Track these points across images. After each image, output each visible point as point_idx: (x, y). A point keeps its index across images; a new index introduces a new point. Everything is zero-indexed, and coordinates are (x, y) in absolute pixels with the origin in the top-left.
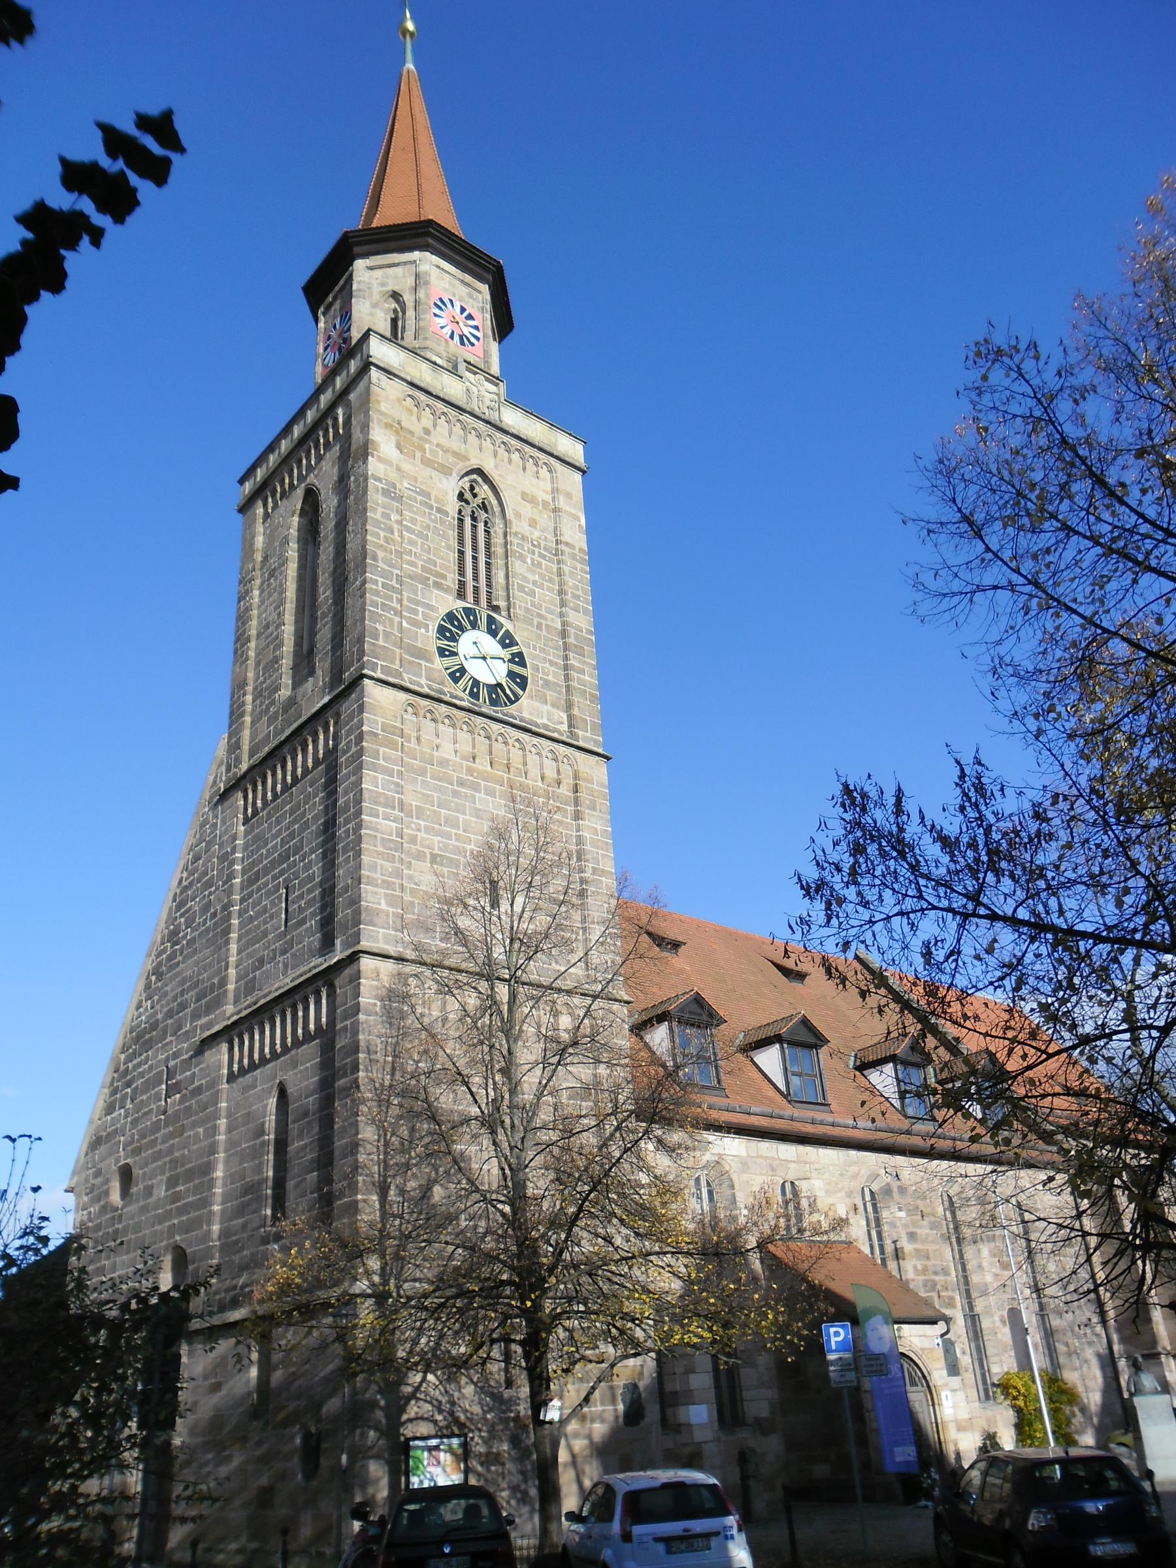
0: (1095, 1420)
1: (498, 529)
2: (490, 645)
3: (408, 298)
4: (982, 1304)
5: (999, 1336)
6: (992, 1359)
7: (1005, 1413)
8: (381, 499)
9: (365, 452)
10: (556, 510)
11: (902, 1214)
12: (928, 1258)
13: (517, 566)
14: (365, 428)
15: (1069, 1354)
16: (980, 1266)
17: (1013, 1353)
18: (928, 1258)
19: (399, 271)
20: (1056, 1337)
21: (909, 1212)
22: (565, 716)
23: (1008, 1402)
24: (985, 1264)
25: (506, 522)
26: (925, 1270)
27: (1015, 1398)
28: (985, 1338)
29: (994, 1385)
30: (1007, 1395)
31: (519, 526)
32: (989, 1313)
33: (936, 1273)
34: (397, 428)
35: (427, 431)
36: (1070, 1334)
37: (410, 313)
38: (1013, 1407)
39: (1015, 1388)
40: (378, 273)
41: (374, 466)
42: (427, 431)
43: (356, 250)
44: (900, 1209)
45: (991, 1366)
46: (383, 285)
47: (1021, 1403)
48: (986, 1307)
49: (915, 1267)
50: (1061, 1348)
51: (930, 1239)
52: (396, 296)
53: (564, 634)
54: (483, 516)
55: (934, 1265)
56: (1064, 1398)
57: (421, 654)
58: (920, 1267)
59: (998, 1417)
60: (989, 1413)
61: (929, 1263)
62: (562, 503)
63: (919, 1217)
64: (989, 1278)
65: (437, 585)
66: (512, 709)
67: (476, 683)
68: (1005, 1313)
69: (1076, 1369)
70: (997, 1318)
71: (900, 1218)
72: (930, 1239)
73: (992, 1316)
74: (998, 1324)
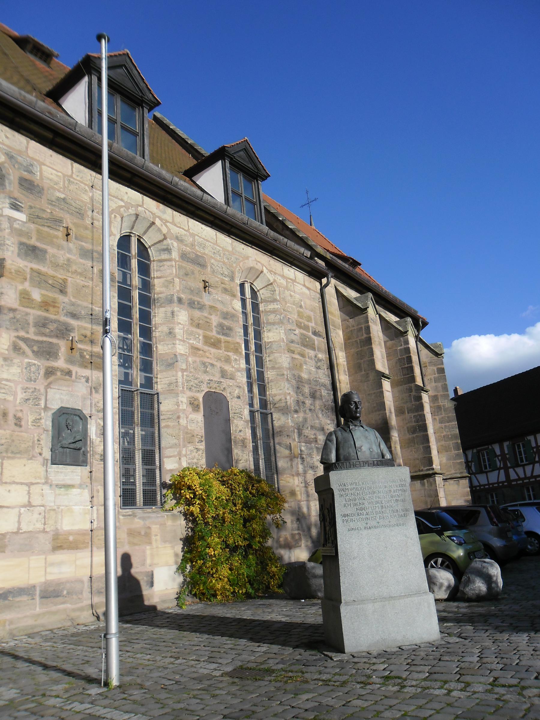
0: (314, 532)
4: (166, 381)
5: (183, 422)
6: (166, 452)
7: (169, 523)
11: (21, 217)
12: (63, 291)
15: (292, 458)
16: (171, 333)
17: (202, 446)
18: (63, 291)
20: (277, 440)
21: (34, 218)
23: (182, 508)
24: (178, 330)
26: (46, 305)
27: (189, 503)
28: (162, 424)
29: (164, 485)
30: (178, 497)
32: (172, 390)
33: (74, 316)
36: (296, 436)
38: (188, 516)
39: (189, 488)
44: (15, 207)
45: (165, 460)
47: (195, 509)
48: (170, 384)
49: (25, 297)
50: (282, 452)
51: (74, 268)
55: (73, 304)
56: (263, 502)
58: (36, 295)
59: (155, 528)
60: (138, 523)
61: (61, 298)
63: (60, 233)
64: (181, 349)
68: (200, 396)
69: (298, 474)
70: (183, 399)
71: (11, 220)
72: (74, 268)
73: (177, 395)
74: (184, 406)
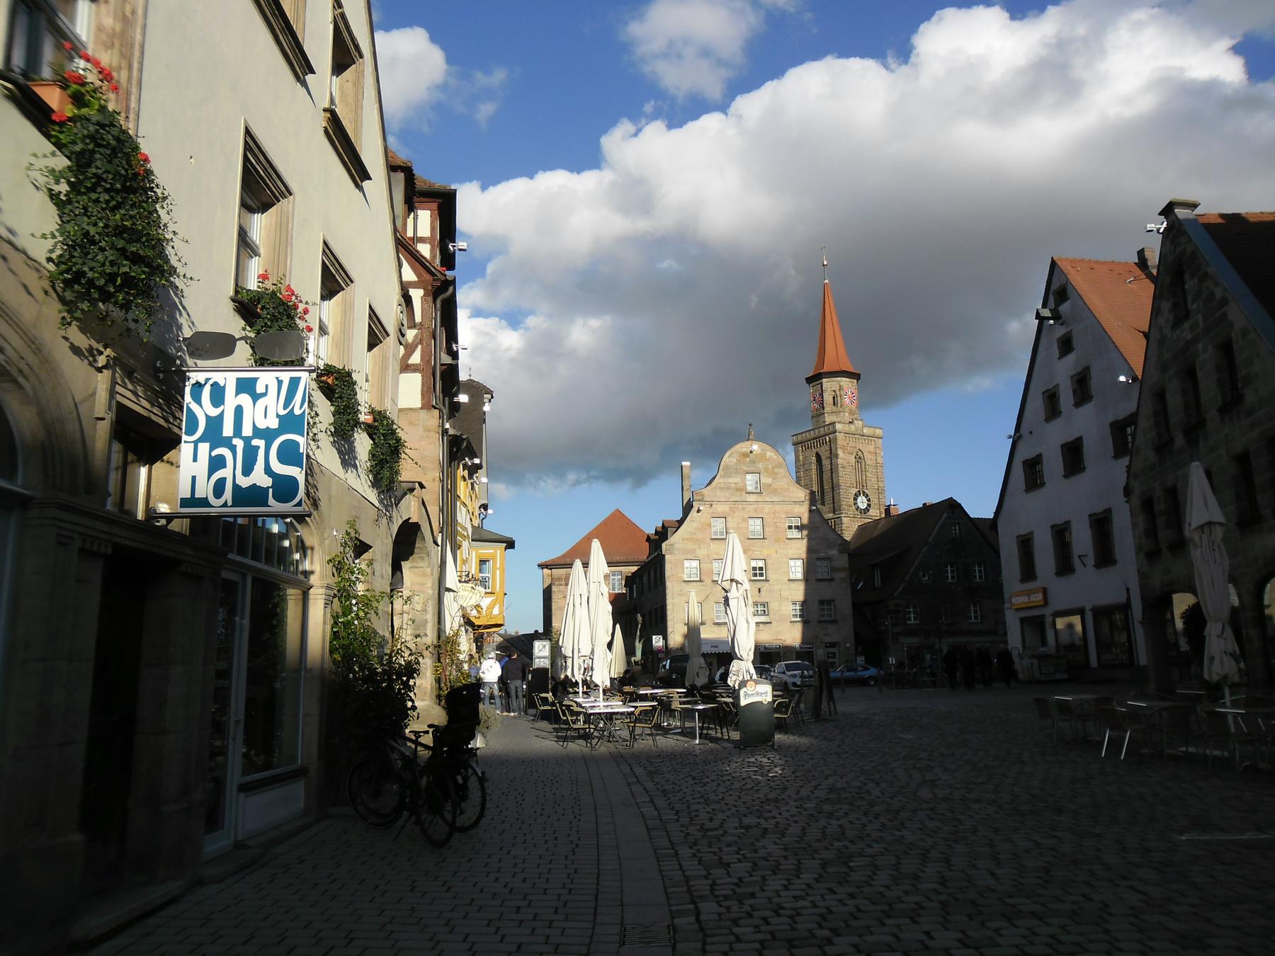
1: (863, 464)
2: (865, 500)
3: (837, 392)
8: (841, 469)
9: (837, 457)
10: (876, 453)
13: (868, 474)
14: (836, 449)
19: (835, 383)
22: (878, 511)
25: (865, 462)
31: (868, 462)
34: (843, 448)
35: (848, 444)
37: (839, 398)
40: (829, 383)
41: (840, 461)
42: (848, 444)
43: (823, 376)
46: (831, 388)
52: (834, 391)
53: (878, 490)
54: (860, 460)
57: (851, 506)
62: (878, 452)
65: (853, 487)
66: (868, 514)
67: (858, 507)
